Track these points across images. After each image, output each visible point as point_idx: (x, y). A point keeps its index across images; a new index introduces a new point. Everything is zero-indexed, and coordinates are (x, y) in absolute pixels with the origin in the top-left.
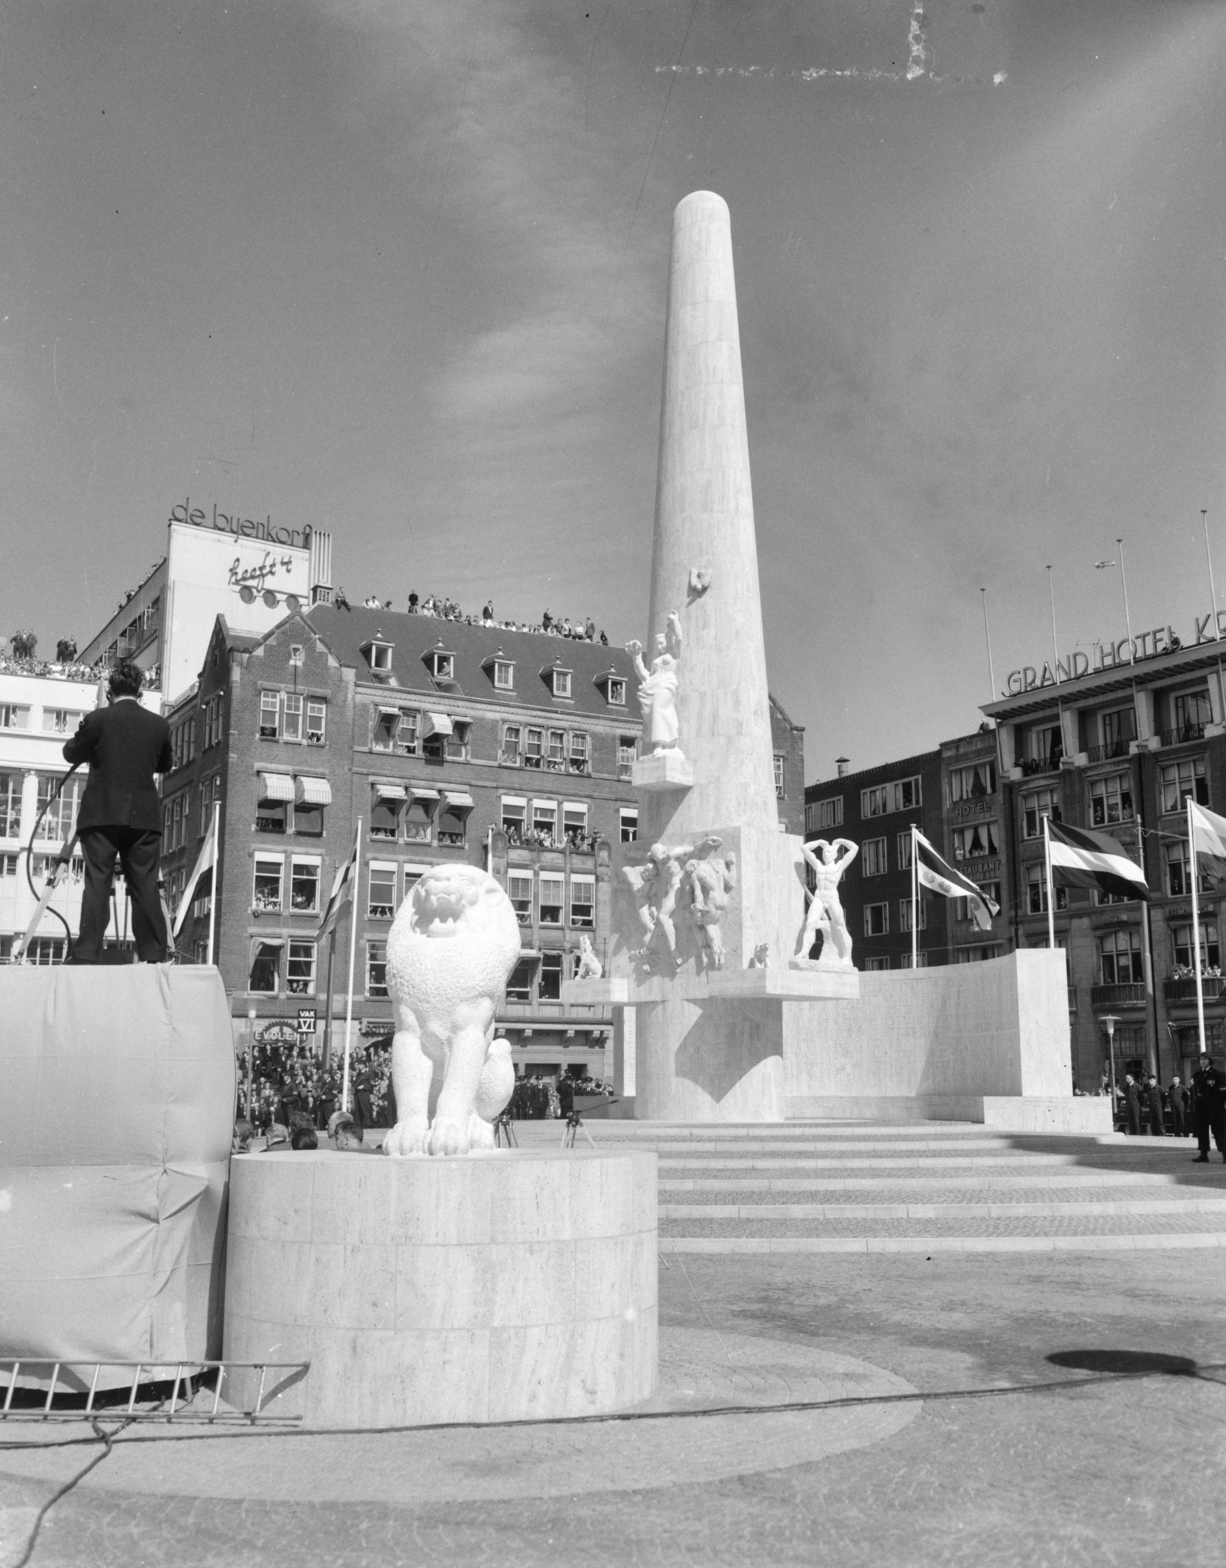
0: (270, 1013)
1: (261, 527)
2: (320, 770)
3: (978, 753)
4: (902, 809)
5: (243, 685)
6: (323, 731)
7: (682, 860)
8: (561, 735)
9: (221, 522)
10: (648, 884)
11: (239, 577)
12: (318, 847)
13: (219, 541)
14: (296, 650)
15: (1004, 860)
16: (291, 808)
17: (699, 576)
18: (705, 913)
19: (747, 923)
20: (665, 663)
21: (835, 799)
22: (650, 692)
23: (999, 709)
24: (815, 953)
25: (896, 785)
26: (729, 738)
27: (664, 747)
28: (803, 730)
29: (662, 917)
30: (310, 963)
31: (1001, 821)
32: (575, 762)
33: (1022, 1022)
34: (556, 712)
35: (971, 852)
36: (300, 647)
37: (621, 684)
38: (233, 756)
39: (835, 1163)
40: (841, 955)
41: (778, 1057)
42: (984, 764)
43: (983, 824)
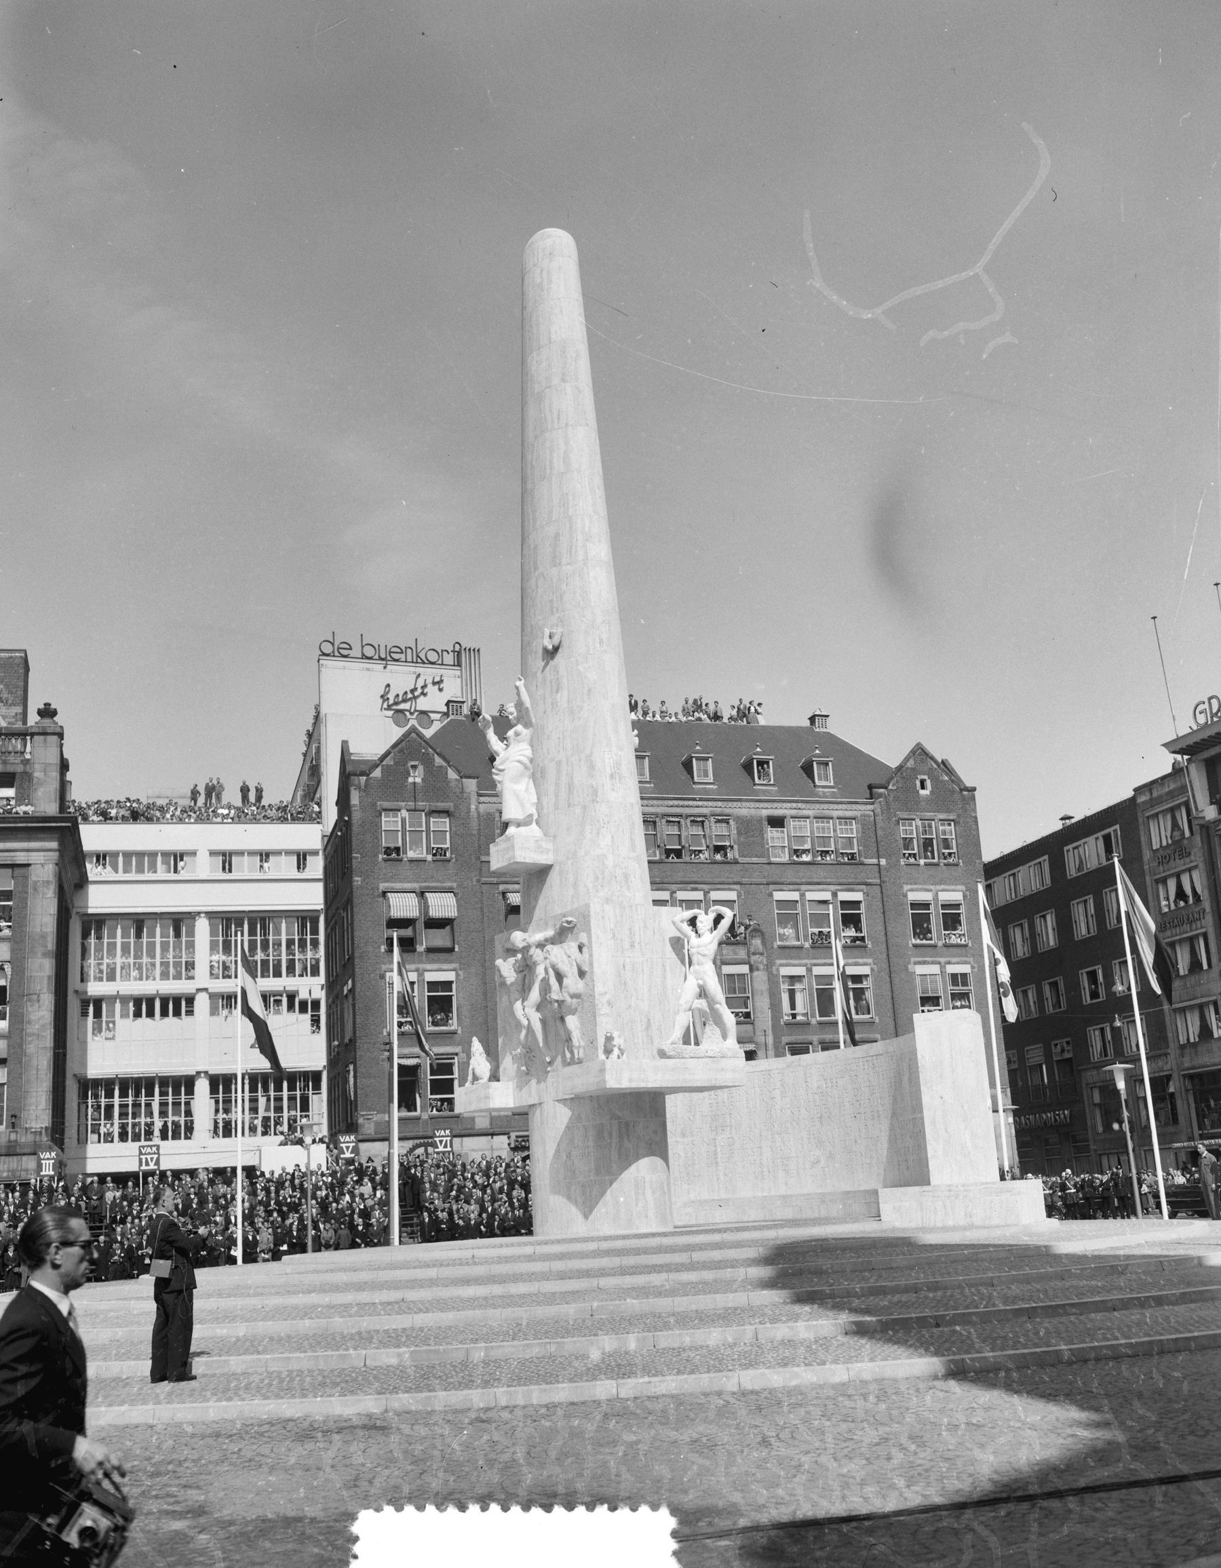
0: (413, 1134)
1: (409, 651)
2: (448, 884)
3: (1171, 795)
4: (1105, 863)
5: (363, 808)
6: (448, 845)
7: (541, 946)
8: (703, 822)
9: (369, 651)
10: (521, 976)
11: (391, 702)
12: (451, 962)
13: (368, 669)
14: (414, 767)
15: (1208, 909)
16: (420, 925)
17: (550, 637)
18: (561, 1003)
19: (603, 1009)
20: (517, 734)
21: (1041, 860)
22: (501, 767)
23: (1183, 745)
24: (690, 1038)
25: (1097, 839)
26: (585, 808)
27: (519, 825)
28: (974, 789)
29: (527, 1012)
30: (452, 1080)
31: (1201, 866)
32: (718, 849)
33: (926, 1099)
34: (694, 799)
35: (1175, 901)
36: (416, 763)
37: (767, 763)
38: (357, 880)
39: (708, 1275)
40: (725, 1037)
41: (658, 1161)
42: (1178, 806)
43: (1184, 871)
